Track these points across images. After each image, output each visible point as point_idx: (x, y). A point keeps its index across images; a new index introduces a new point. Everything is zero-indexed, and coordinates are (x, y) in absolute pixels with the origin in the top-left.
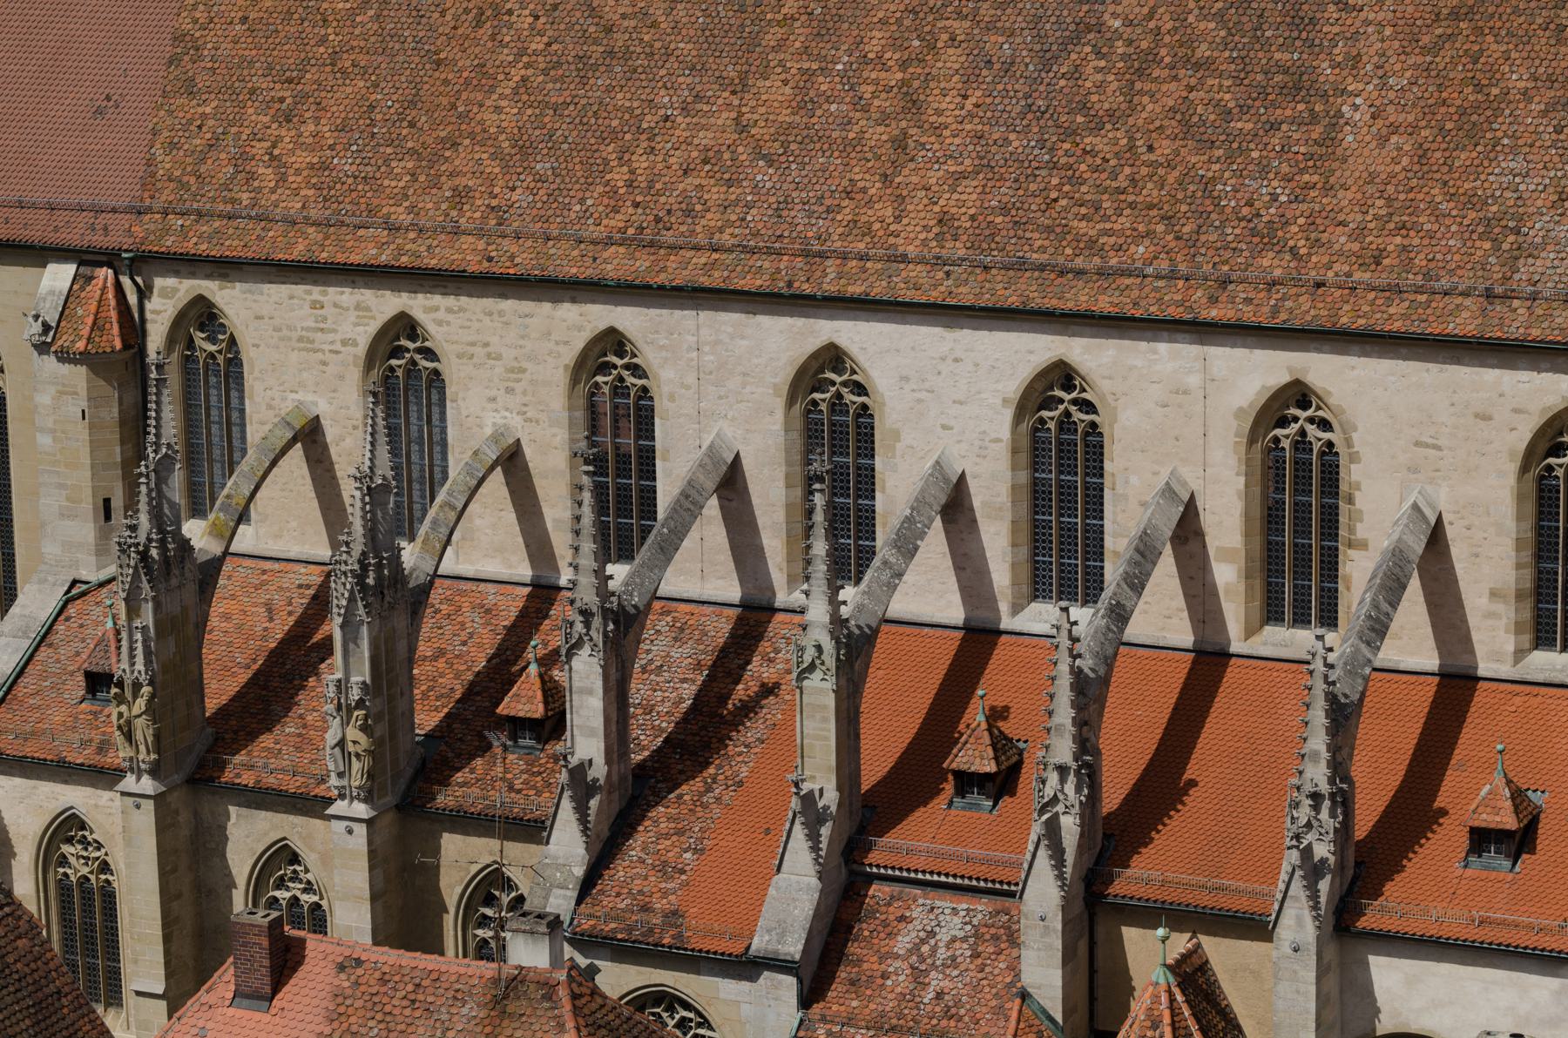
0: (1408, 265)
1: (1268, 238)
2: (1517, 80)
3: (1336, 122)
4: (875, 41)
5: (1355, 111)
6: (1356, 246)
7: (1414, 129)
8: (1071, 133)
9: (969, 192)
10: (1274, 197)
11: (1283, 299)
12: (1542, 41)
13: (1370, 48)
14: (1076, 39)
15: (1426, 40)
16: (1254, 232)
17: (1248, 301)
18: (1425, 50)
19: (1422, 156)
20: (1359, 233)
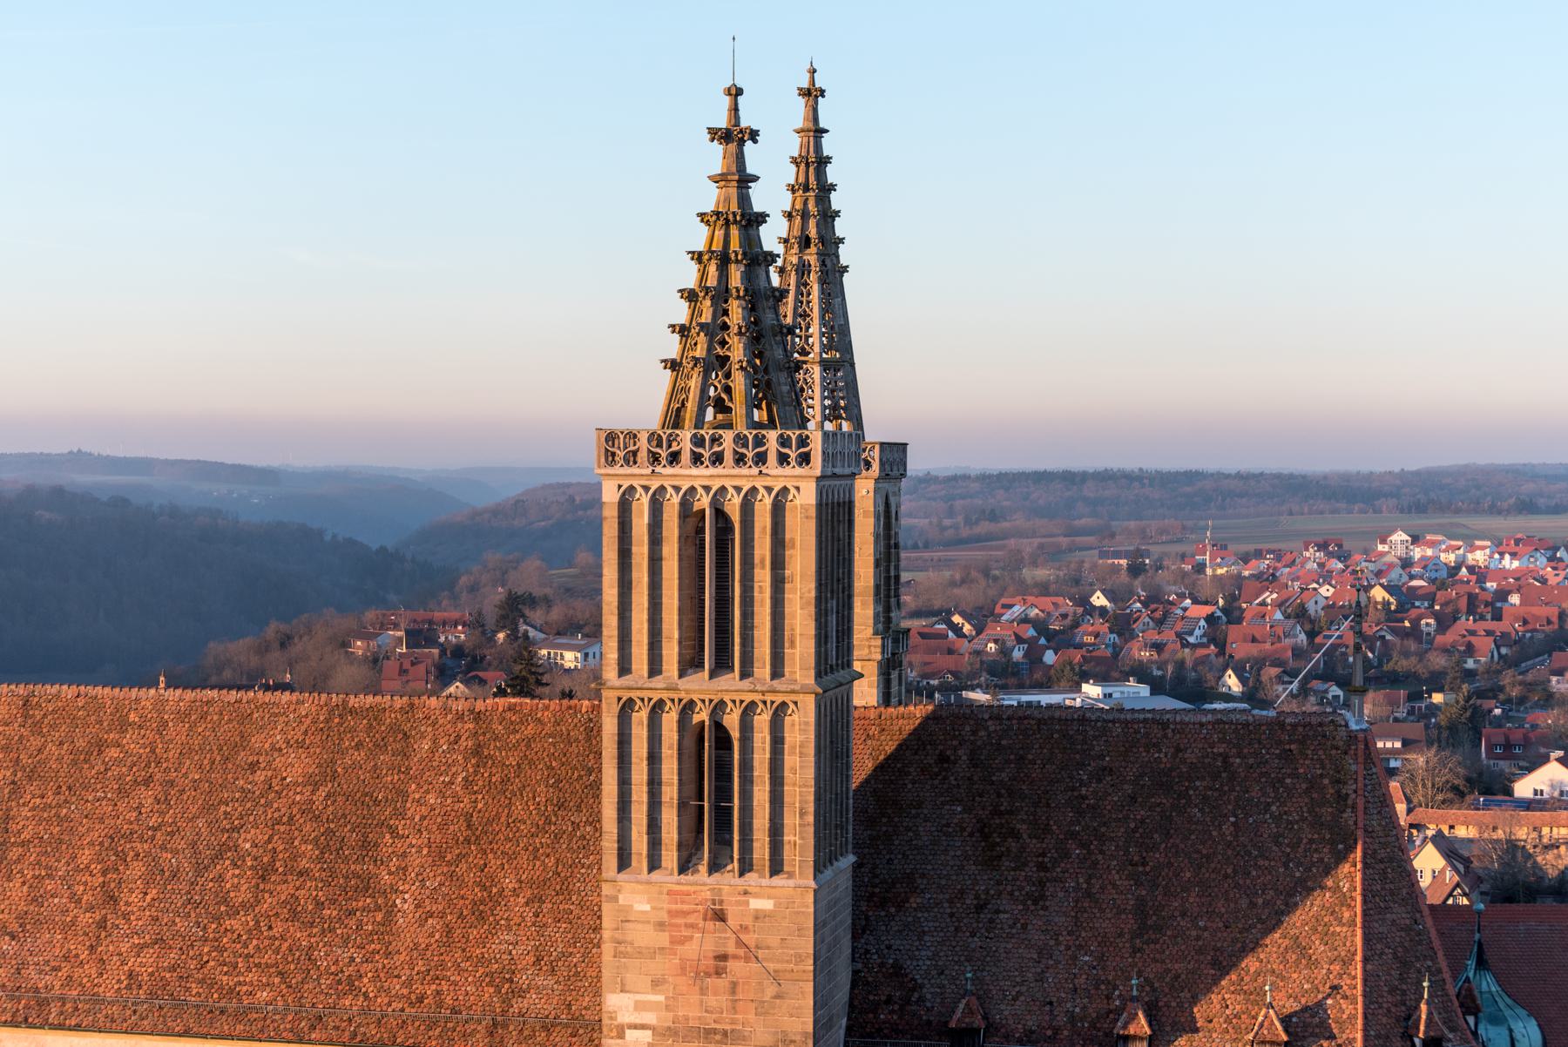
0: (440, 1005)
1: (352, 986)
2: (509, 883)
3: (391, 910)
4: (85, 857)
5: (404, 903)
6: (405, 991)
7: (442, 915)
8: (217, 919)
9: (148, 956)
10: (352, 959)
11: (359, 1026)
12: (524, 858)
13: (415, 861)
14: (219, 856)
15: (449, 857)
16: (339, 982)
17: (336, 1028)
18: (449, 864)
19: (449, 931)
20: (409, 983)
